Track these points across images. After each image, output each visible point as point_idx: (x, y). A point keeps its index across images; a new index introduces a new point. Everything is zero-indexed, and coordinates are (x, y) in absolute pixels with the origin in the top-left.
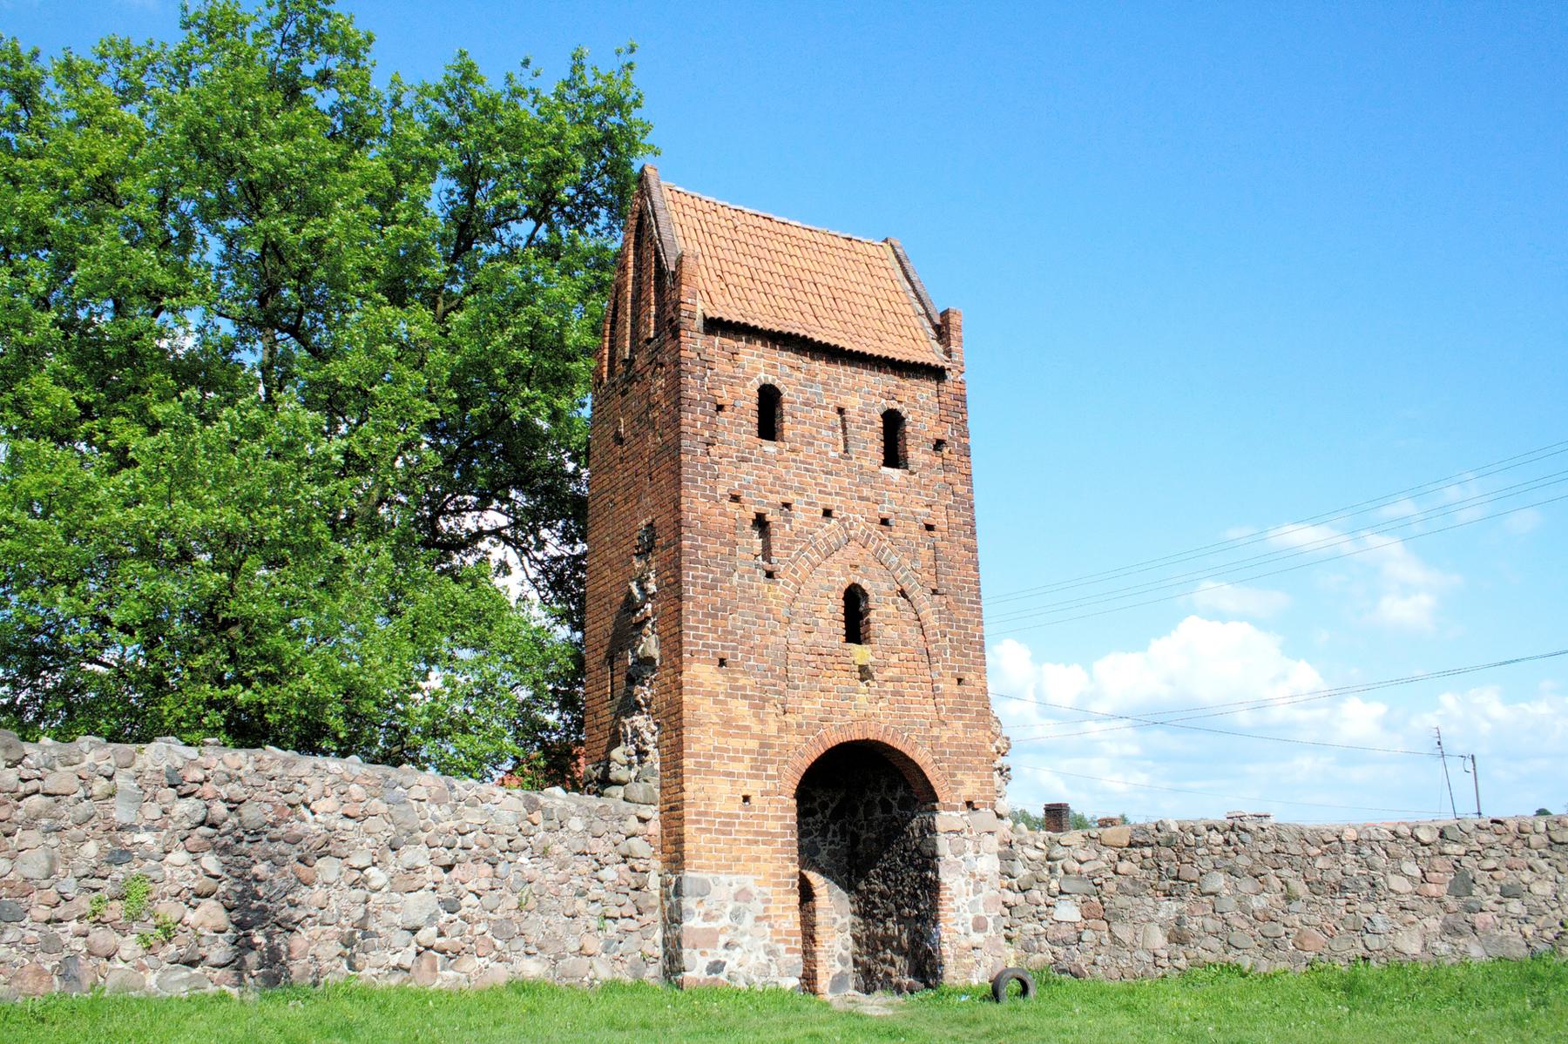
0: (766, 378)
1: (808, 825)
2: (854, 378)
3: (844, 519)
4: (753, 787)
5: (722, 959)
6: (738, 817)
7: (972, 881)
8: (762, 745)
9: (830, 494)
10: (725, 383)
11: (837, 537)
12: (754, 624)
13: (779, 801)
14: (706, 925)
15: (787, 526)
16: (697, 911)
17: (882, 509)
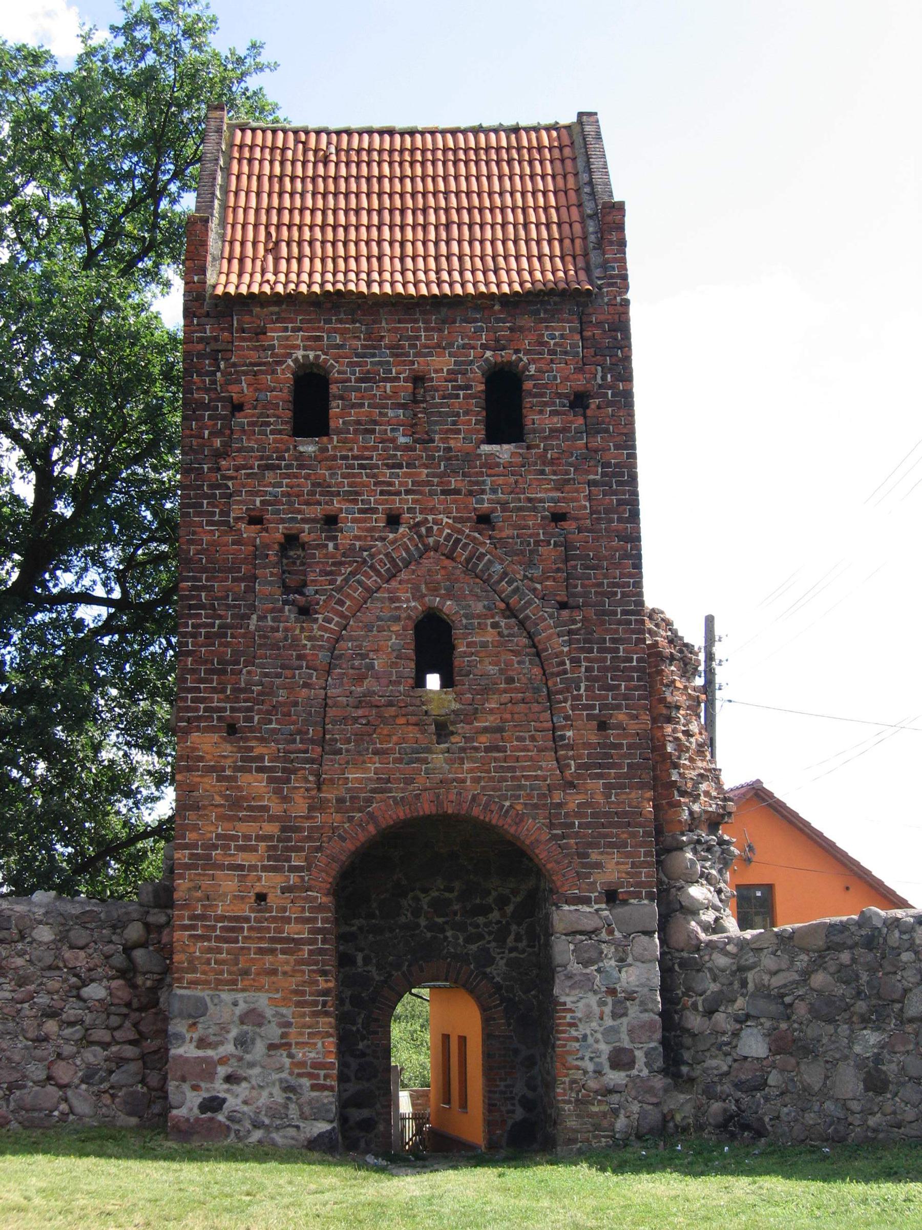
0: (306, 357)
1: (477, 926)
2: (440, 330)
3: (418, 525)
4: (268, 882)
5: (222, 1095)
6: (247, 920)
7: (609, 1000)
8: (284, 829)
9: (398, 493)
10: (245, 373)
11: (407, 550)
12: (278, 675)
13: (307, 899)
14: (201, 1053)
15: (331, 545)
16: (188, 1036)
17: (481, 501)
